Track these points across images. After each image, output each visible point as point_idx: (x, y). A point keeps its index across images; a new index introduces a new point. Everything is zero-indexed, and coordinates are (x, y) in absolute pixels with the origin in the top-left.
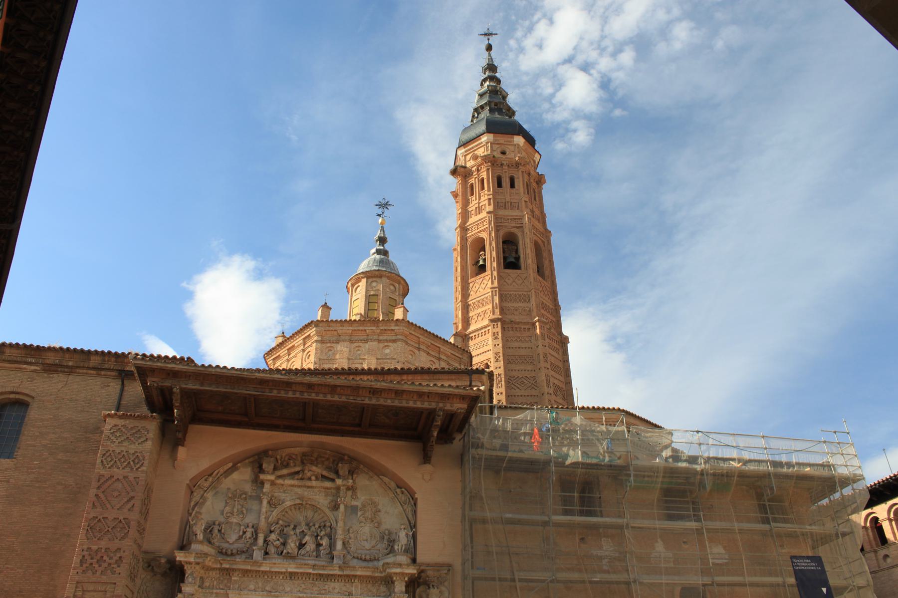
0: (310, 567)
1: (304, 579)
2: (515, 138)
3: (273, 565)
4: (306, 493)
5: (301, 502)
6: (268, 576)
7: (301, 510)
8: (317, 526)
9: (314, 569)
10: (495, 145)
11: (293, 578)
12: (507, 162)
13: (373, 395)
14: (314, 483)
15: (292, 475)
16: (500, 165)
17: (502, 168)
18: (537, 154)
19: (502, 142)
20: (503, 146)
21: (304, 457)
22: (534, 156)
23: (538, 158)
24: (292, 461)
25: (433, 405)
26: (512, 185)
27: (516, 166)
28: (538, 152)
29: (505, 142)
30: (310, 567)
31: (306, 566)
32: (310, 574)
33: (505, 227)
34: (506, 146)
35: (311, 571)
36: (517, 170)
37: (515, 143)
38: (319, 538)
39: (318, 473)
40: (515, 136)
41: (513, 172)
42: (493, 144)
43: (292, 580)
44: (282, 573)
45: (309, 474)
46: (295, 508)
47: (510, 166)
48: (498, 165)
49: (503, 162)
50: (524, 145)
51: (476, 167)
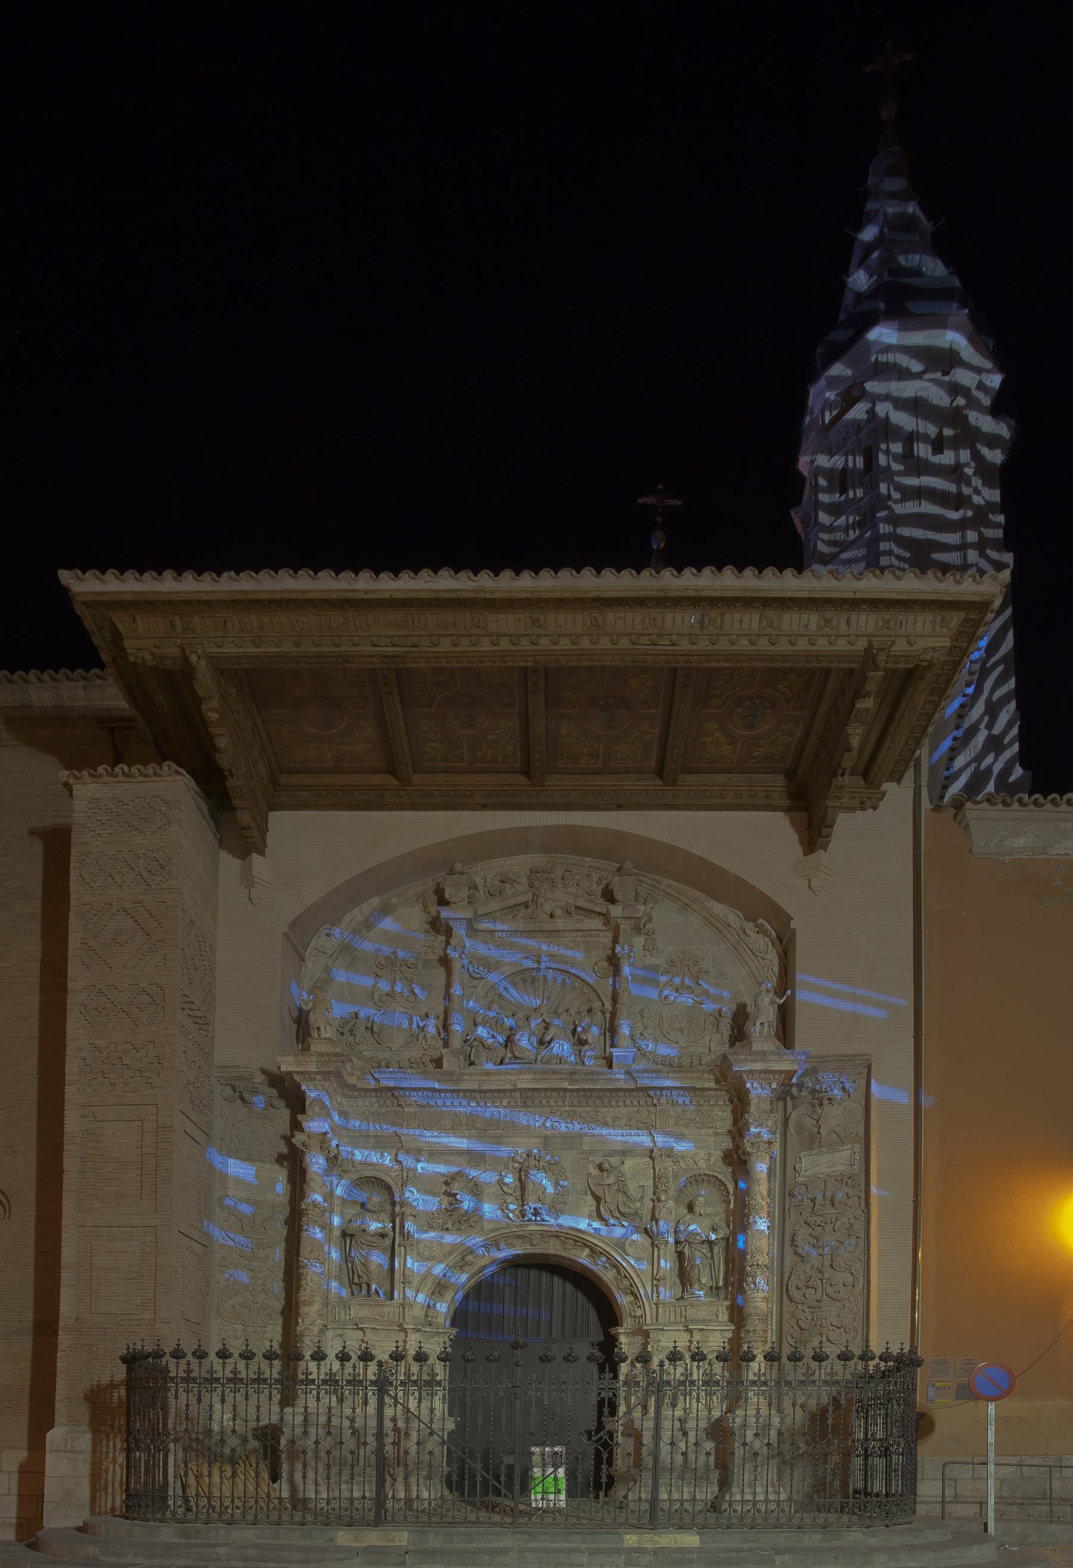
0: (564, 1076)
1: (552, 1103)
3: (483, 1078)
4: (544, 947)
5: (535, 966)
6: (478, 1103)
7: (536, 983)
8: (573, 1012)
9: (572, 1081)
11: (529, 1103)
14: (561, 924)
15: (511, 910)
21: (533, 876)
24: (507, 885)
30: (564, 1076)
31: (555, 1076)
32: (565, 1090)
35: (566, 1085)
38: (579, 1029)
39: (567, 903)
43: (529, 1106)
44: (505, 1091)
45: (547, 907)
46: (524, 981)
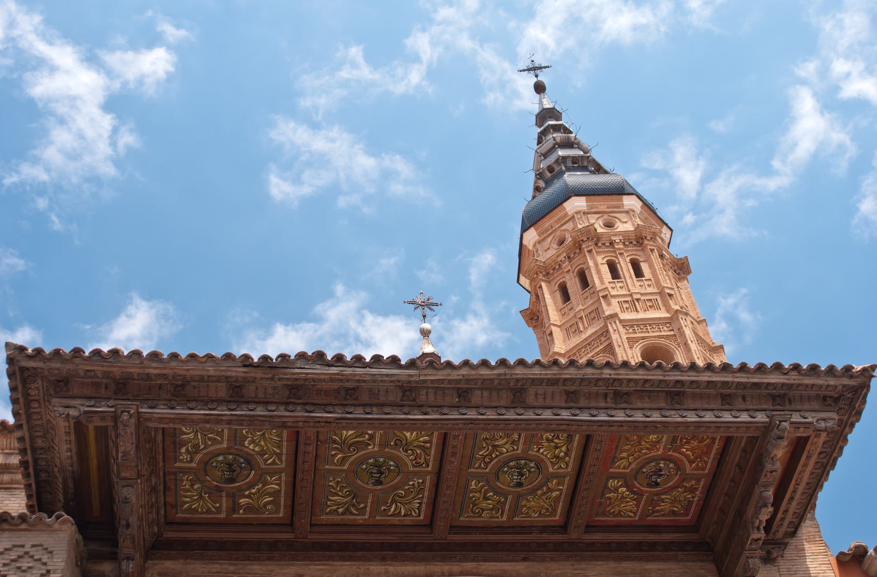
2: (624, 198)
10: (592, 215)
12: (621, 238)
13: (616, 403)
16: (607, 244)
17: (614, 247)
18: (665, 230)
19: (603, 208)
20: (606, 217)
22: (661, 232)
23: (668, 236)
25: (761, 417)
26: (639, 273)
27: (638, 242)
28: (666, 225)
29: (608, 208)
33: (643, 338)
34: (611, 215)
36: (640, 248)
37: (626, 208)
40: (624, 196)
41: (634, 253)
42: (588, 213)
47: (627, 243)
48: (604, 244)
49: (613, 238)
50: (641, 212)
51: (565, 254)
